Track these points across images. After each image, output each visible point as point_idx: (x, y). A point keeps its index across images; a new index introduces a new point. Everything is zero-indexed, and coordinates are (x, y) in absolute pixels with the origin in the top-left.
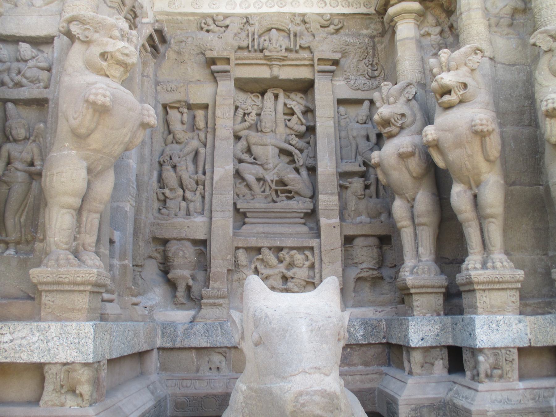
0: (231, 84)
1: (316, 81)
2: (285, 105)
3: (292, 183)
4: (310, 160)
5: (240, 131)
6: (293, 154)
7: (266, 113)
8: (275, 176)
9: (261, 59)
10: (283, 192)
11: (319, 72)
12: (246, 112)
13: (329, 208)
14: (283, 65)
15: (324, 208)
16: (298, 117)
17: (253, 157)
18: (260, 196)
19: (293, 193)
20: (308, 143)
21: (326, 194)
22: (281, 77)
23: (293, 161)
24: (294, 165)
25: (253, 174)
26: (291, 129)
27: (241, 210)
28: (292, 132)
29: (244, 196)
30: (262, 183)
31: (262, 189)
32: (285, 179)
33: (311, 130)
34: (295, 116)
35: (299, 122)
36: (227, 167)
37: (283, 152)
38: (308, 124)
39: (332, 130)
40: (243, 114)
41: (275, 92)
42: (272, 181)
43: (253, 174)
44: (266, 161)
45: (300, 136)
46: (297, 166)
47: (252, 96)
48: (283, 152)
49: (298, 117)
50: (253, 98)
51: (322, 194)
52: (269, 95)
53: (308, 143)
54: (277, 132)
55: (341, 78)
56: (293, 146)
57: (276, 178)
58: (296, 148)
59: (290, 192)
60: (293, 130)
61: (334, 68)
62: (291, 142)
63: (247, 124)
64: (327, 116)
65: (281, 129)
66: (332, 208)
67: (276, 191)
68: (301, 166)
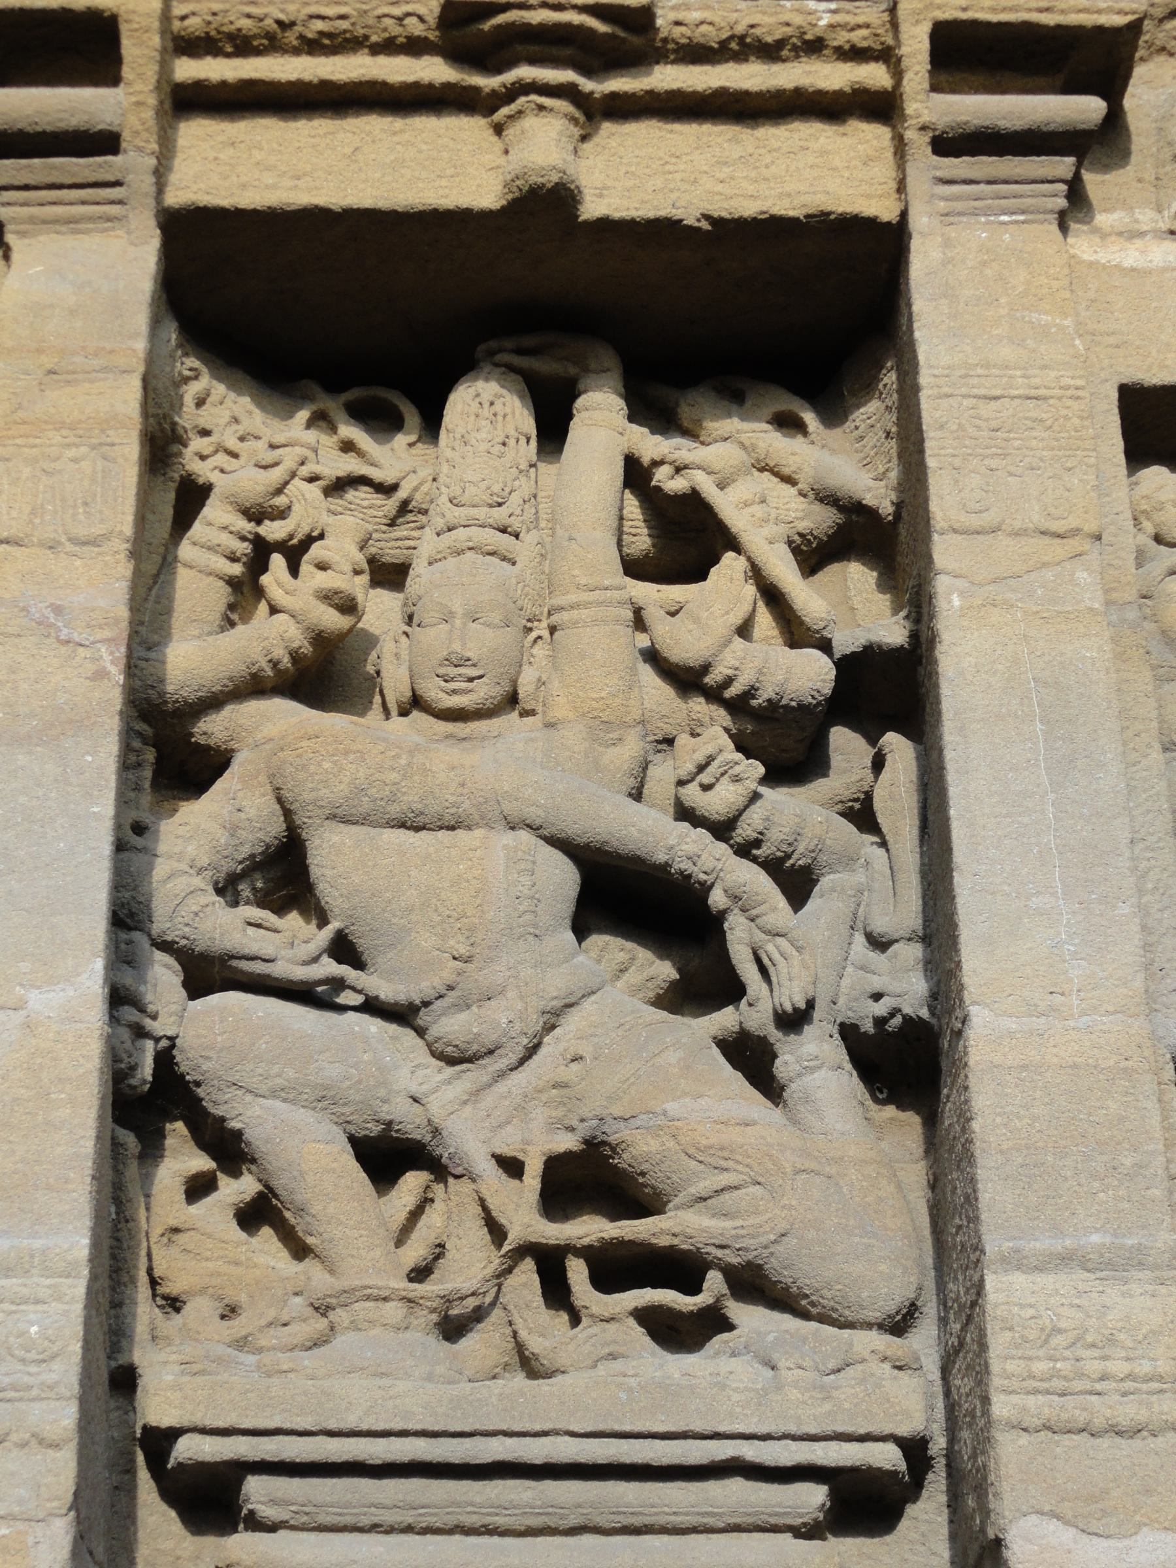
0: (124, 262)
1: (919, 222)
2: (636, 474)
3: (703, 1186)
4: (874, 956)
5: (213, 702)
6: (717, 899)
7: (461, 533)
8: (540, 1115)
9: (414, 47)
10: (616, 1268)
11: (947, 144)
12: (273, 531)
13: (1103, 1410)
14: (623, 109)
15: (1039, 1407)
16: (756, 573)
17: (328, 932)
18: (394, 1311)
19: (714, 1282)
20: (862, 815)
21: (1066, 1260)
22: (592, 208)
23: (705, 981)
24: (725, 1019)
25: (324, 1099)
26: (687, 680)
27: (187, 1449)
28: (699, 706)
29: (230, 1312)
30: (413, 1182)
31: (415, 1252)
32: (642, 1148)
33: (890, 691)
34: (730, 566)
35: (765, 621)
36: (38, 1001)
37: (623, 896)
38: (846, 641)
39: (1092, 650)
40: (244, 548)
41: (543, 366)
42: (512, 1167)
43: (324, 1099)
44: (448, 971)
45: (785, 743)
46: (755, 1014)
47: (333, 406)
48: (623, 896)
49: (756, 573)
50: (349, 431)
51: (1016, 1262)
52: (486, 408)
53: (862, 815)
54: (561, 709)
55: (1146, 218)
56: (722, 829)
57: (544, 1140)
58: (745, 850)
59: (682, 1269)
60: (714, 695)
61: (1087, 108)
62: (692, 795)
63: (270, 637)
64: (1036, 518)
65: (594, 670)
66: (1128, 1412)
67: (550, 1264)
68: (793, 1021)
